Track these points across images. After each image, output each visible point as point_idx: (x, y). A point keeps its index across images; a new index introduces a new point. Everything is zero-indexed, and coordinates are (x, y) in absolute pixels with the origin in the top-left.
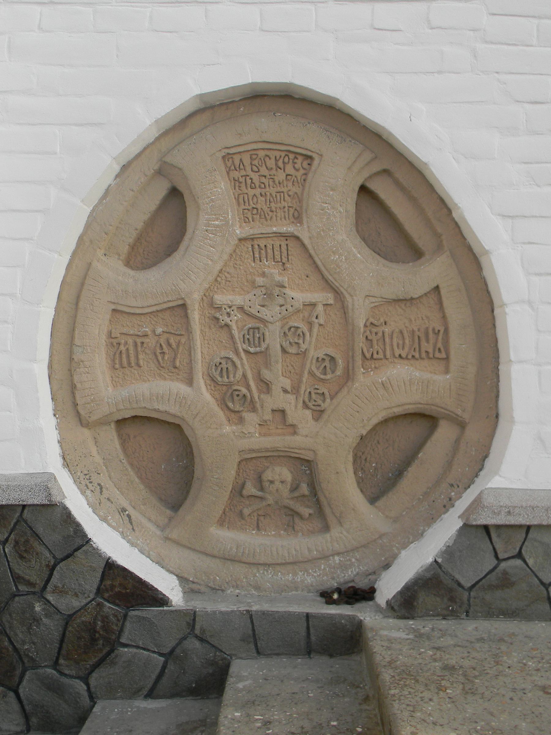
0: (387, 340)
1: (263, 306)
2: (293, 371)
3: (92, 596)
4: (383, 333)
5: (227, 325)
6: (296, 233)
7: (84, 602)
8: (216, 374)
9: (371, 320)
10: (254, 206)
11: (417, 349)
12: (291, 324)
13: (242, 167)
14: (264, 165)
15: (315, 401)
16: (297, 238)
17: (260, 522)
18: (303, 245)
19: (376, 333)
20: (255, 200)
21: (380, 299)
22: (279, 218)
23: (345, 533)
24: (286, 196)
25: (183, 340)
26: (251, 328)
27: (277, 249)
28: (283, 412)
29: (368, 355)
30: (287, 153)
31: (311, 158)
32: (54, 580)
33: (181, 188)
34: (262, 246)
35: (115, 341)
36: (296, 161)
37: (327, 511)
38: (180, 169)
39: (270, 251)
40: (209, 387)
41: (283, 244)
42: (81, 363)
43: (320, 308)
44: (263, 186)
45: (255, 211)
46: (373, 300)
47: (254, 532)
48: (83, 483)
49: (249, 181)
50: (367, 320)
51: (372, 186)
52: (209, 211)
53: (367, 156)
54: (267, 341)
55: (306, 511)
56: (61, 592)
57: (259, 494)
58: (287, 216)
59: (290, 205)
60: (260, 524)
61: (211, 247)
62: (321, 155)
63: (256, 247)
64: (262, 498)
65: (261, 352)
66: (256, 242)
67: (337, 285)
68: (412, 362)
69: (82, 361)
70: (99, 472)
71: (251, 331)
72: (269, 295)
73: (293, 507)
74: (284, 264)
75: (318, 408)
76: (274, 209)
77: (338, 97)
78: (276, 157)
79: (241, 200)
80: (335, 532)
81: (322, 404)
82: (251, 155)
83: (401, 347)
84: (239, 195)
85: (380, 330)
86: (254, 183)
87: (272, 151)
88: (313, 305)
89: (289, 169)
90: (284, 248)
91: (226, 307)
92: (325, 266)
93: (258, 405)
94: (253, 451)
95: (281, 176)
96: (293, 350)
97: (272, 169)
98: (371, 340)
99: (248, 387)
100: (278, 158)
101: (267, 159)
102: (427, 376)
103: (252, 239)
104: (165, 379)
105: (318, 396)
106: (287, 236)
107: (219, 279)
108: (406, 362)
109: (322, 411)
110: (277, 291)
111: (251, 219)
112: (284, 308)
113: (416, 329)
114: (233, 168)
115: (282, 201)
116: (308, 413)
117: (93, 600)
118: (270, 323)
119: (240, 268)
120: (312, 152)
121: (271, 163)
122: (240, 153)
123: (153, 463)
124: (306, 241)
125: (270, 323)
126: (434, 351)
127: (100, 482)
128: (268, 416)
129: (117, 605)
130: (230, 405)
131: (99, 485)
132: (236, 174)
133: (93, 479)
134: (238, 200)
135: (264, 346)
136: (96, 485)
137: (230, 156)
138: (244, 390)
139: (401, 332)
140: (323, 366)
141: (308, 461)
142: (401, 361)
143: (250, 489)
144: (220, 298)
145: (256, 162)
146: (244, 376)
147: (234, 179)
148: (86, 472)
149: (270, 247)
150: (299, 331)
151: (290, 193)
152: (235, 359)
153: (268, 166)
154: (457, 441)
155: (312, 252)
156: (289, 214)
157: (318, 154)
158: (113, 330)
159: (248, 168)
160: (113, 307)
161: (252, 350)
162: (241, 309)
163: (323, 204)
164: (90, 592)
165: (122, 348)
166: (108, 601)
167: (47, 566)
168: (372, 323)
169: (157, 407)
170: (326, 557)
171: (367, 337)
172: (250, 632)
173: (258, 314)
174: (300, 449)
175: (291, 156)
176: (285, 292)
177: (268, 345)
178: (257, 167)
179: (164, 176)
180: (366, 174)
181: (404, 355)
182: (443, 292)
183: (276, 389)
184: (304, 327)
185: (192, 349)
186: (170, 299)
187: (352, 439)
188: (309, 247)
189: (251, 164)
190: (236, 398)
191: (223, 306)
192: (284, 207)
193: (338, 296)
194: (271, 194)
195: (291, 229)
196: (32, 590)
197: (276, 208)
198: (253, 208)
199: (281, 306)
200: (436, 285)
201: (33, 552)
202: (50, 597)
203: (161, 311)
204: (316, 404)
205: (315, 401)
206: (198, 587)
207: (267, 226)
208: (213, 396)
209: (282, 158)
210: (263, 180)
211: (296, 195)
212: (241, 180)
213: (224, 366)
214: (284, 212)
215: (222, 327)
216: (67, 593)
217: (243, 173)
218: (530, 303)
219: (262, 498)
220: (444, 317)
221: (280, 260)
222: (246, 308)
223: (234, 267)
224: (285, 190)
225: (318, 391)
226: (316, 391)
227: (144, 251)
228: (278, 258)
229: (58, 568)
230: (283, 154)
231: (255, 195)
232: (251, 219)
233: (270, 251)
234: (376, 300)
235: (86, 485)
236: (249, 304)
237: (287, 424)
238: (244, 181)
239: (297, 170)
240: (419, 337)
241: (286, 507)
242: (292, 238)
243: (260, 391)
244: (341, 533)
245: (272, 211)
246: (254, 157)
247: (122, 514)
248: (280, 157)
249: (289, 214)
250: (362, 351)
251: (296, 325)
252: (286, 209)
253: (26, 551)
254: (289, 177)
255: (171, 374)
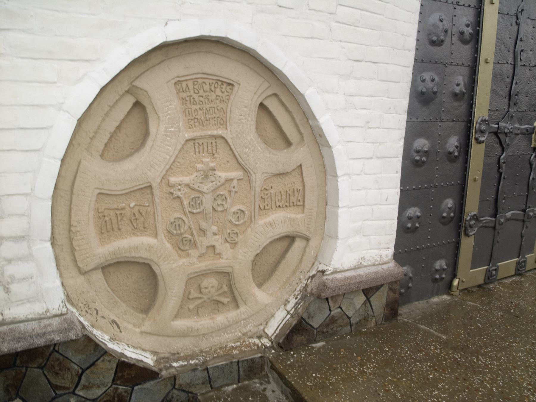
0: (273, 198)
1: (201, 183)
2: (219, 221)
3: (109, 385)
4: (271, 193)
5: (178, 197)
6: (223, 135)
7: (104, 389)
8: (171, 228)
9: (265, 187)
10: (196, 117)
11: (288, 202)
12: (219, 193)
13: (187, 90)
14: (202, 89)
15: (232, 238)
16: (223, 138)
17: (199, 311)
18: (227, 142)
19: (267, 194)
20: (196, 113)
21: (270, 174)
22: (211, 125)
23: (248, 308)
24: (216, 110)
25: (149, 209)
26: (193, 198)
27: (210, 145)
28: (214, 247)
29: (262, 208)
30: (216, 81)
31: (232, 85)
32: (82, 382)
33: (145, 103)
34: (201, 143)
35: (101, 215)
36: (222, 86)
37: (238, 298)
38: (146, 91)
39: (205, 147)
40: (167, 237)
41: (214, 141)
42: (78, 233)
43: (235, 182)
44: (201, 103)
45: (196, 120)
46: (266, 175)
47: (196, 317)
48: (84, 310)
49: (192, 100)
50: (262, 187)
51: (265, 103)
52: (167, 121)
53: (266, 85)
54: (204, 205)
55: (225, 300)
56: (86, 388)
57: (200, 295)
58: (216, 123)
59: (218, 116)
60: (199, 312)
61: (168, 146)
62: (239, 84)
63: (197, 144)
64: (200, 298)
65: (200, 212)
66: (196, 141)
67: (247, 167)
68: (285, 208)
69: (78, 231)
70: (95, 301)
71: (194, 199)
72: (206, 177)
73: (218, 300)
74: (213, 154)
75: (234, 242)
76: (208, 119)
77: (256, 49)
78: (210, 84)
79: (187, 113)
80: (242, 309)
81: (236, 239)
82: (193, 82)
83: (280, 201)
84: (185, 109)
86: (195, 101)
87: (207, 80)
88: (232, 180)
89: (218, 92)
90: (214, 144)
91: (177, 185)
92: (240, 156)
93: (198, 245)
94: (197, 272)
95: (213, 96)
96: (220, 209)
97: (207, 91)
98: (264, 199)
99: (192, 234)
100: (211, 84)
101: (204, 85)
102: (293, 216)
103: (194, 140)
104: (138, 236)
105: (234, 235)
106: (215, 137)
107: (172, 167)
108: (282, 209)
109: (236, 243)
110: (211, 173)
111: (193, 126)
112: (214, 183)
113: (288, 190)
114: (181, 90)
115: (213, 114)
116: (228, 244)
117: (111, 386)
118: (206, 193)
119: (186, 159)
120: (234, 81)
121: (207, 87)
122: (186, 80)
123: (128, 287)
124: (229, 141)
125: (206, 193)
126: (297, 201)
127: (96, 307)
129: (127, 386)
130: (182, 248)
131: (96, 309)
132: (184, 95)
133: (90, 306)
134: (184, 112)
135: (202, 208)
136: (93, 309)
137: (179, 82)
139: (280, 192)
140: (237, 216)
141: (228, 273)
142: (279, 209)
143: (194, 294)
144: (173, 180)
145: (196, 87)
146: (190, 228)
147: (182, 98)
148: (85, 303)
149: (205, 144)
150: (224, 197)
151: (218, 108)
152: (184, 218)
153: (205, 89)
154: (305, 248)
155: (232, 147)
156: (217, 122)
157: (237, 83)
158: (100, 207)
159: (192, 91)
160: (99, 191)
161: (195, 211)
162: (188, 185)
163: (240, 117)
164: (108, 383)
165: (107, 219)
166: (121, 385)
167: (77, 375)
168: (265, 189)
169: (134, 255)
170: (237, 323)
171: (262, 197)
172: (207, 378)
173: (199, 189)
174: (224, 267)
175: (220, 83)
176: (215, 173)
177: (205, 207)
178: (197, 90)
179: (131, 94)
180: (264, 96)
181: (281, 206)
182: (303, 168)
183: (209, 234)
184: (227, 194)
185: (156, 215)
186: (141, 183)
187: (250, 257)
188: (231, 144)
189: (194, 88)
190: (185, 242)
191: (176, 185)
192: (215, 118)
193: (246, 173)
194: (206, 109)
196: (67, 391)
197: (209, 118)
198: (195, 118)
199: (212, 182)
200: (300, 164)
201: (65, 369)
202: (81, 393)
203: (134, 191)
204: (233, 239)
205: (232, 238)
206: (164, 354)
207: (204, 130)
208: (170, 243)
209: (213, 85)
210: (201, 99)
211: (222, 110)
212: (188, 99)
213: (177, 223)
214: (215, 121)
215: (175, 198)
216: (92, 387)
217: (188, 94)
219: (200, 298)
220: (303, 182)
221: (211, 152)
222: (191, 185)
223: (183, 158)
224: (215, 106)
225: (234, 232)
226: (233, 232)
227: (114, 146)
228: (210, 151)
229: (84, 374)
230: (214, 82)
231: (196, 109)
232: (193, 126)
233: (205, 147)
234: (268, 175)
235: (86, 311)
236: (193, 182)
237: (216, 253)
238: (189, 100)
239: (223, 92)
240: (289, 194)
241: (213, 300)
242: (220, 138)
243: (199, 236)
244: (246, 309)
245: (207, 120)
246: (196, 83)
247: (112, 324)
248: (213, 83)
249: (217, 122)
250: (259, 206)
251: (221, 193)
252: (216, 119)
253: (60, 370)
254: (217, 97)
255: (141, 232)
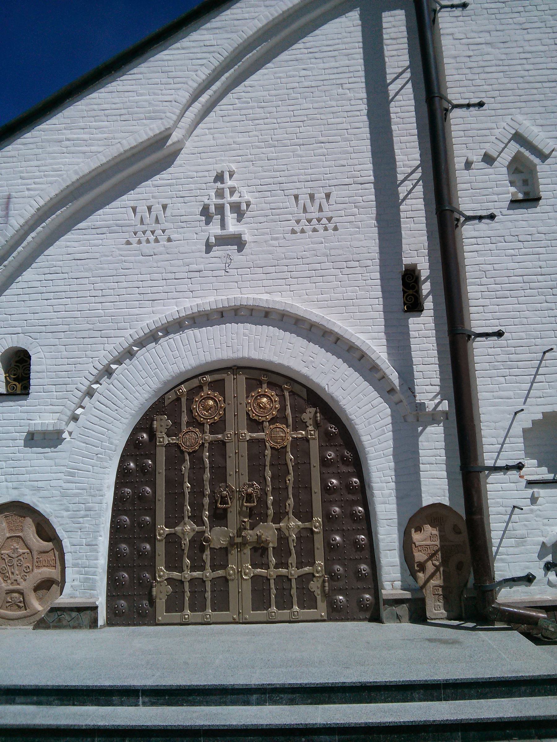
64: (11, 602)
72: (14, 551)
85: (40, 559)
88: (24, 553)
128: (13, 581)
132: (8, 521)
138: (8, 575)
162: (7, 554)
184: (23, 559)
195: (20, 534)
218: (71, 552)
